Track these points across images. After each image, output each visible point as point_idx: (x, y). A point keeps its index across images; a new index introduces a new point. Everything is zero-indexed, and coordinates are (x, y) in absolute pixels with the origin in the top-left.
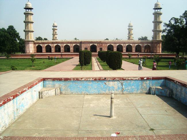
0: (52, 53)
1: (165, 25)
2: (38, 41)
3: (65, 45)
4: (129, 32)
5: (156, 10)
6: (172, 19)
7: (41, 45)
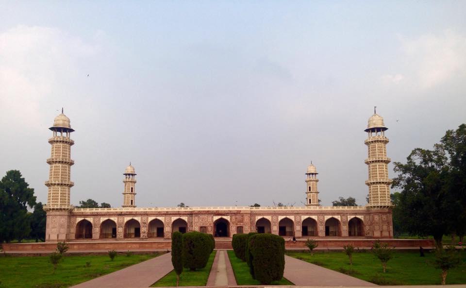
0: (117, 240)
1: (397, 168)
2: (82, 210)
3: (151, 219)
4: (310, 187)
5: (374, 134)
6: (414, 153)
7: (90, 219)
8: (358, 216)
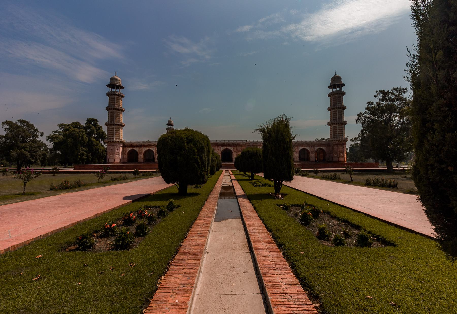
5: (334, 90)
7: (137, 149)
8: (321, 147)
